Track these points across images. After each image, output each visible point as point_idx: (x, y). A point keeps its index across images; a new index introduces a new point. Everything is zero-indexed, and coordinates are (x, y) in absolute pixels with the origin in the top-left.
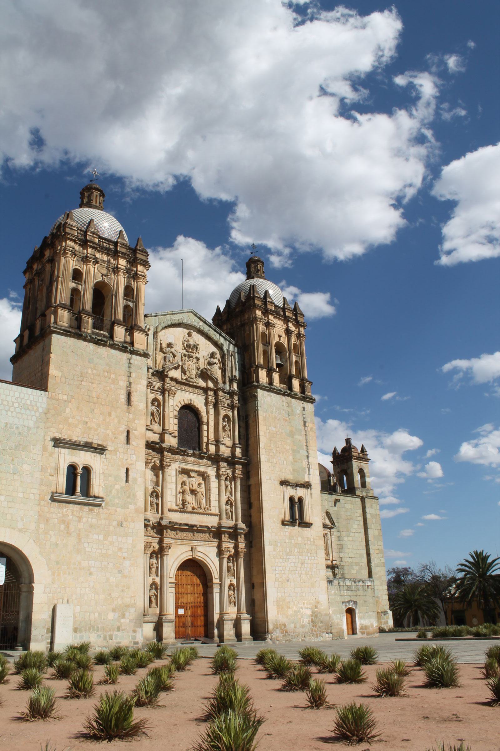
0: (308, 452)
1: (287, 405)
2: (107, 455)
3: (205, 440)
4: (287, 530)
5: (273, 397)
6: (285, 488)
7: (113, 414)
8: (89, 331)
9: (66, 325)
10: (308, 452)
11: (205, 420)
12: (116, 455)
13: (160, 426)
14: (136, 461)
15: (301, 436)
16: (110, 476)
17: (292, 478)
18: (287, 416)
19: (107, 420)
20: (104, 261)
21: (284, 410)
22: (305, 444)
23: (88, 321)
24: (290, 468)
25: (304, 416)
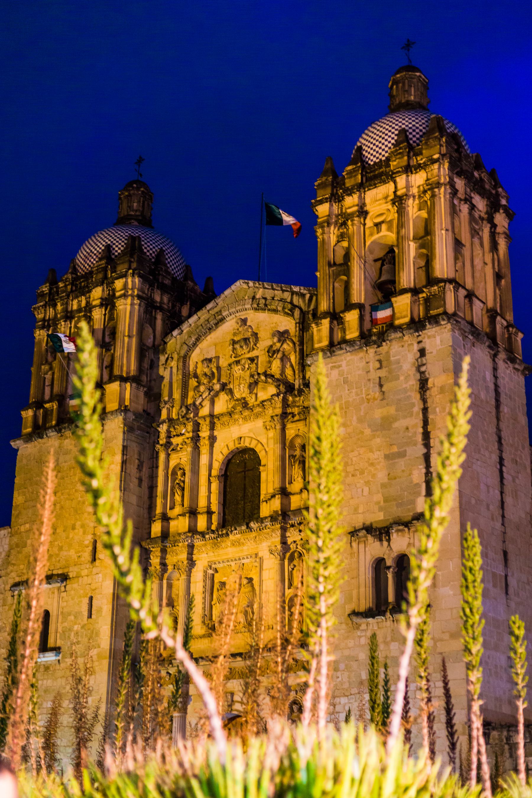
0: (427, 445)
1: (377, 365)
2: (67, 587)
3: (262, 497)
4: (363, 634)
5: (344, 367)
6: (362, 546)
7: (78, 524)
8: (54, 423)
9: (29, 430)
10: (427, 445)
11: (263, 463)
12: (78, 581)
13: (183, 506)
14: (103, 581)
15: (411, 415)
16: (69, 614)
17: (382, 518)
18: (377, 388)
19: (71, 536)
20: (79, 310)
21: (369, 380)
22: (421, 430)
23: (53, 410)
24: (379, 497)
25: (423, 369)
